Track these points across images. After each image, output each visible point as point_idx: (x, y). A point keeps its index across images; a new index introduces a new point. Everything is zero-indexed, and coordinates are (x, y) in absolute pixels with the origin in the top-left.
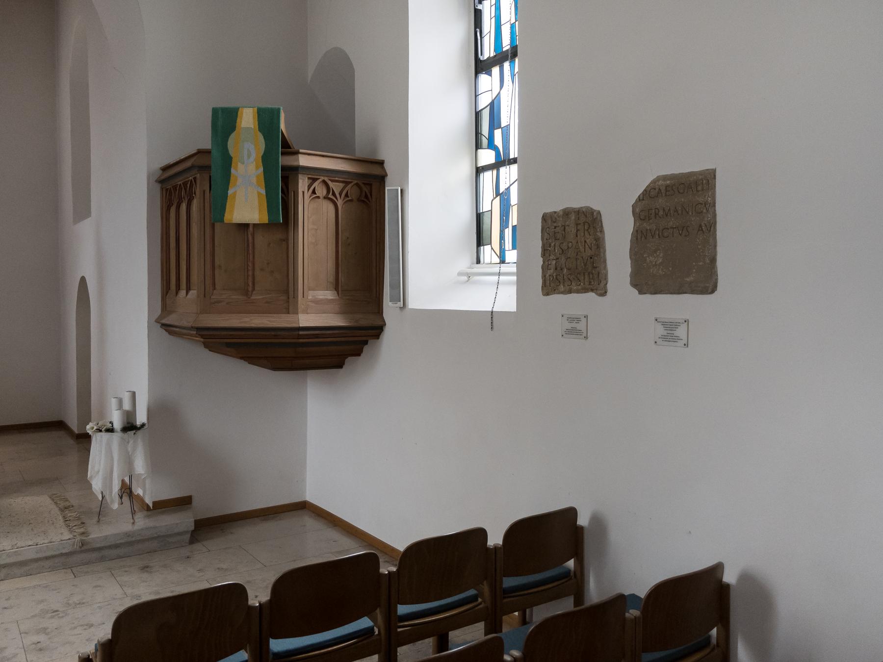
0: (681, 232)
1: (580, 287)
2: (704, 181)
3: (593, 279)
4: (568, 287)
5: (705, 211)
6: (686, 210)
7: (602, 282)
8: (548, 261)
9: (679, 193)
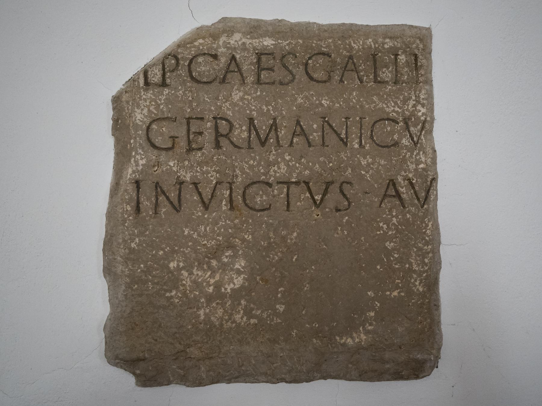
0: (318, 198)
2: (402, 58)
5: (405, 142)
6: (338, 135)
9: (311, 78)
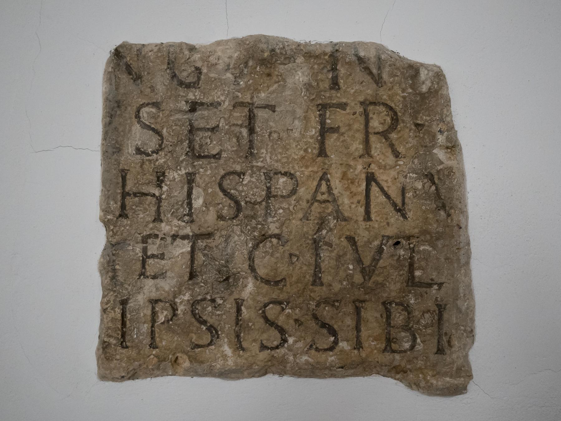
1: (331, 358)
3: (406, 328)
4: (265, 354)
7: (455, 343)
8: (145, 240)
